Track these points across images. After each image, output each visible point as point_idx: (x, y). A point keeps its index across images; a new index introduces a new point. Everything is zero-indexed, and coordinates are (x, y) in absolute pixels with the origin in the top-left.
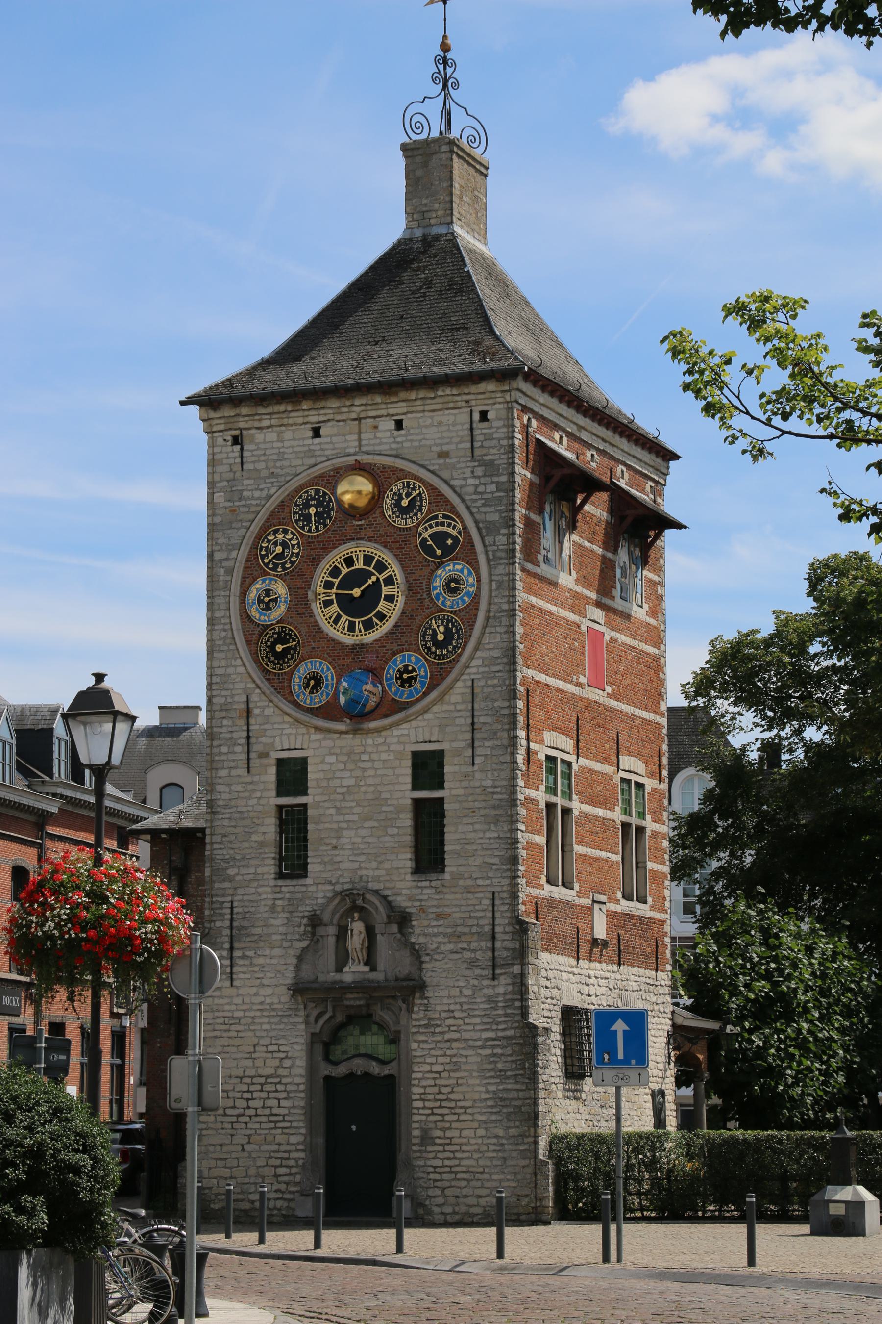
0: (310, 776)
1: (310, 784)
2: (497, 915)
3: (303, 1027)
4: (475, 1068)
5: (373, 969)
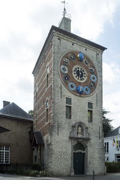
0: (72, 102)
1: (72, 103)
5: (83, 136)
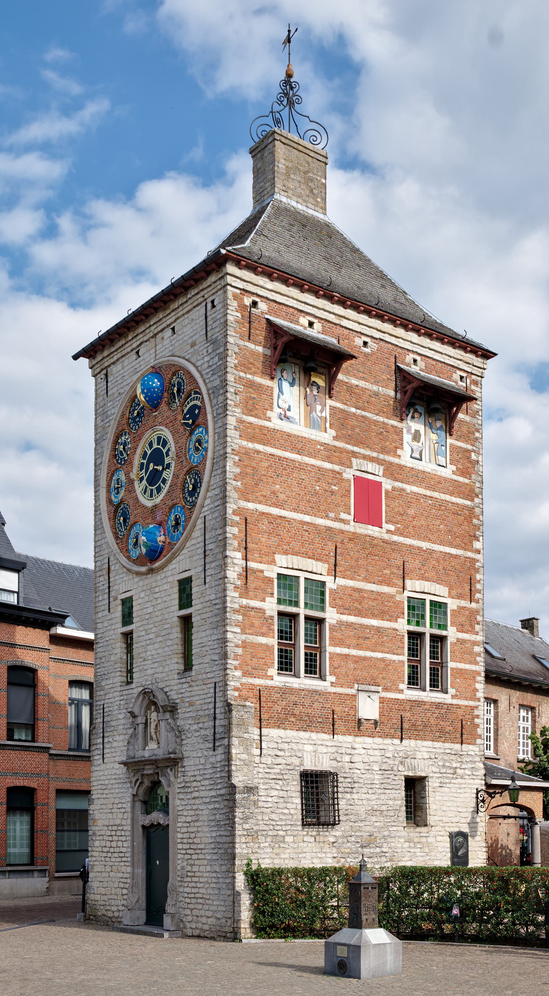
2: (217, 700)
3: (131, 790)
4: (206, 819)
